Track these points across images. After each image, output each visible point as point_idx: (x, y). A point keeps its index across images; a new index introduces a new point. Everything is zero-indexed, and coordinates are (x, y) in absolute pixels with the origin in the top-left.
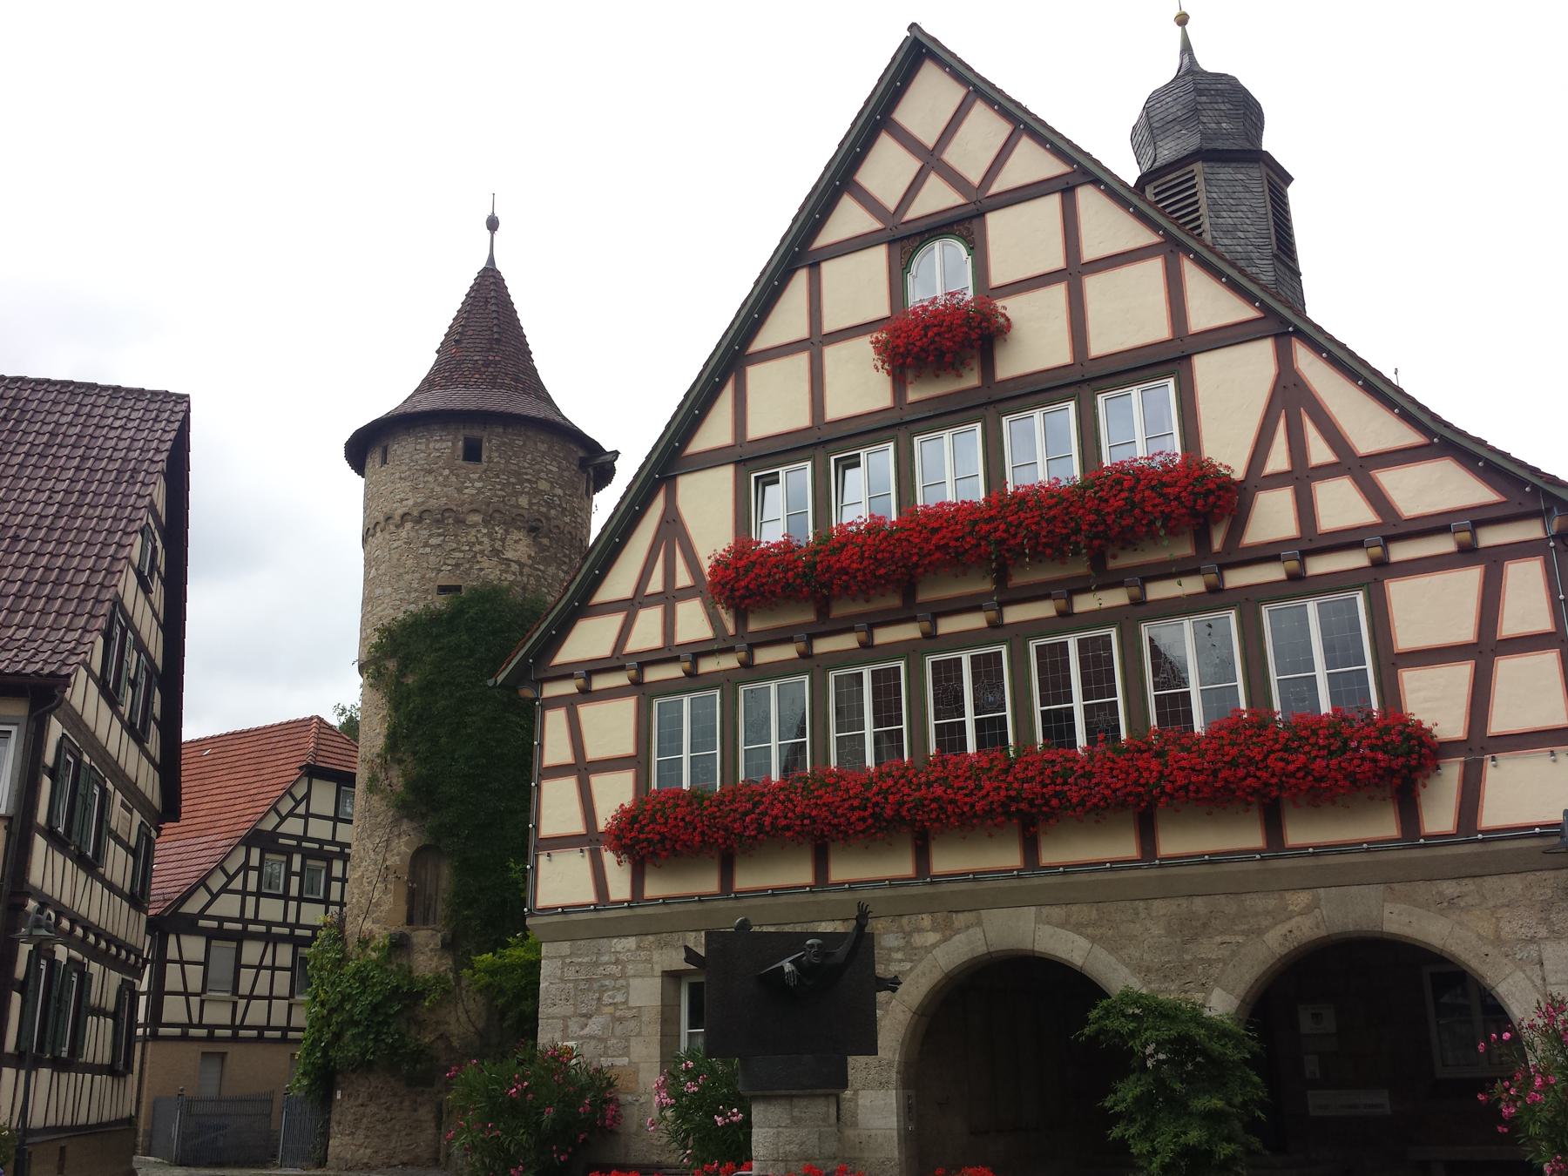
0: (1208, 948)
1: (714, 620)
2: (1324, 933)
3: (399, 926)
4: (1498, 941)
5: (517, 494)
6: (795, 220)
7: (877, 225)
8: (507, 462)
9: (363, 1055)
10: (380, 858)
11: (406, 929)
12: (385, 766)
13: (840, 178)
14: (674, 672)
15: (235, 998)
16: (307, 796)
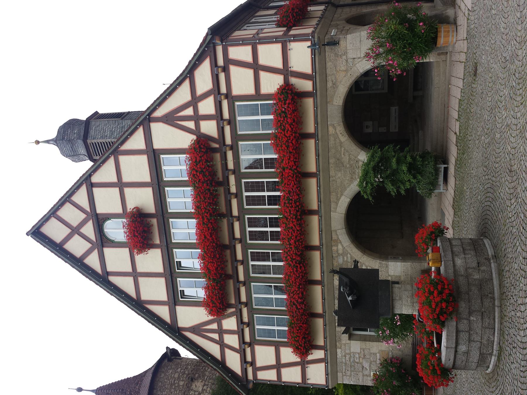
0: (345, 159)
2: (342, 123)
4: (346, 71)
5: (179, 386)
6: (91, 280)
7: (96, 251)
8: (167, 389)
13: (78, 263)
14: (247, 331)
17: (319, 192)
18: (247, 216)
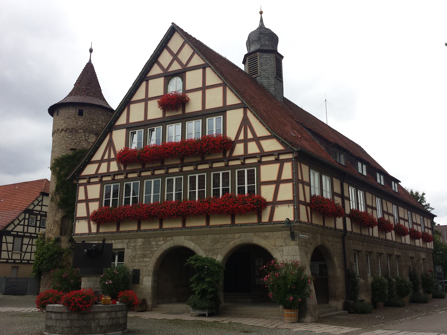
0: (218, 246)
1: (119, 168)
3: (58, 235)
4: (275, 246)
5: (92, 125)
6: (143, 69)
7: (162, 72)
9: (48, 267)
10: (53, 218)
11: (60, 236)
12: (55, 195)
14: (109, 178)
16: (42, 200)
17: (197, 227)
18: (205, 174)
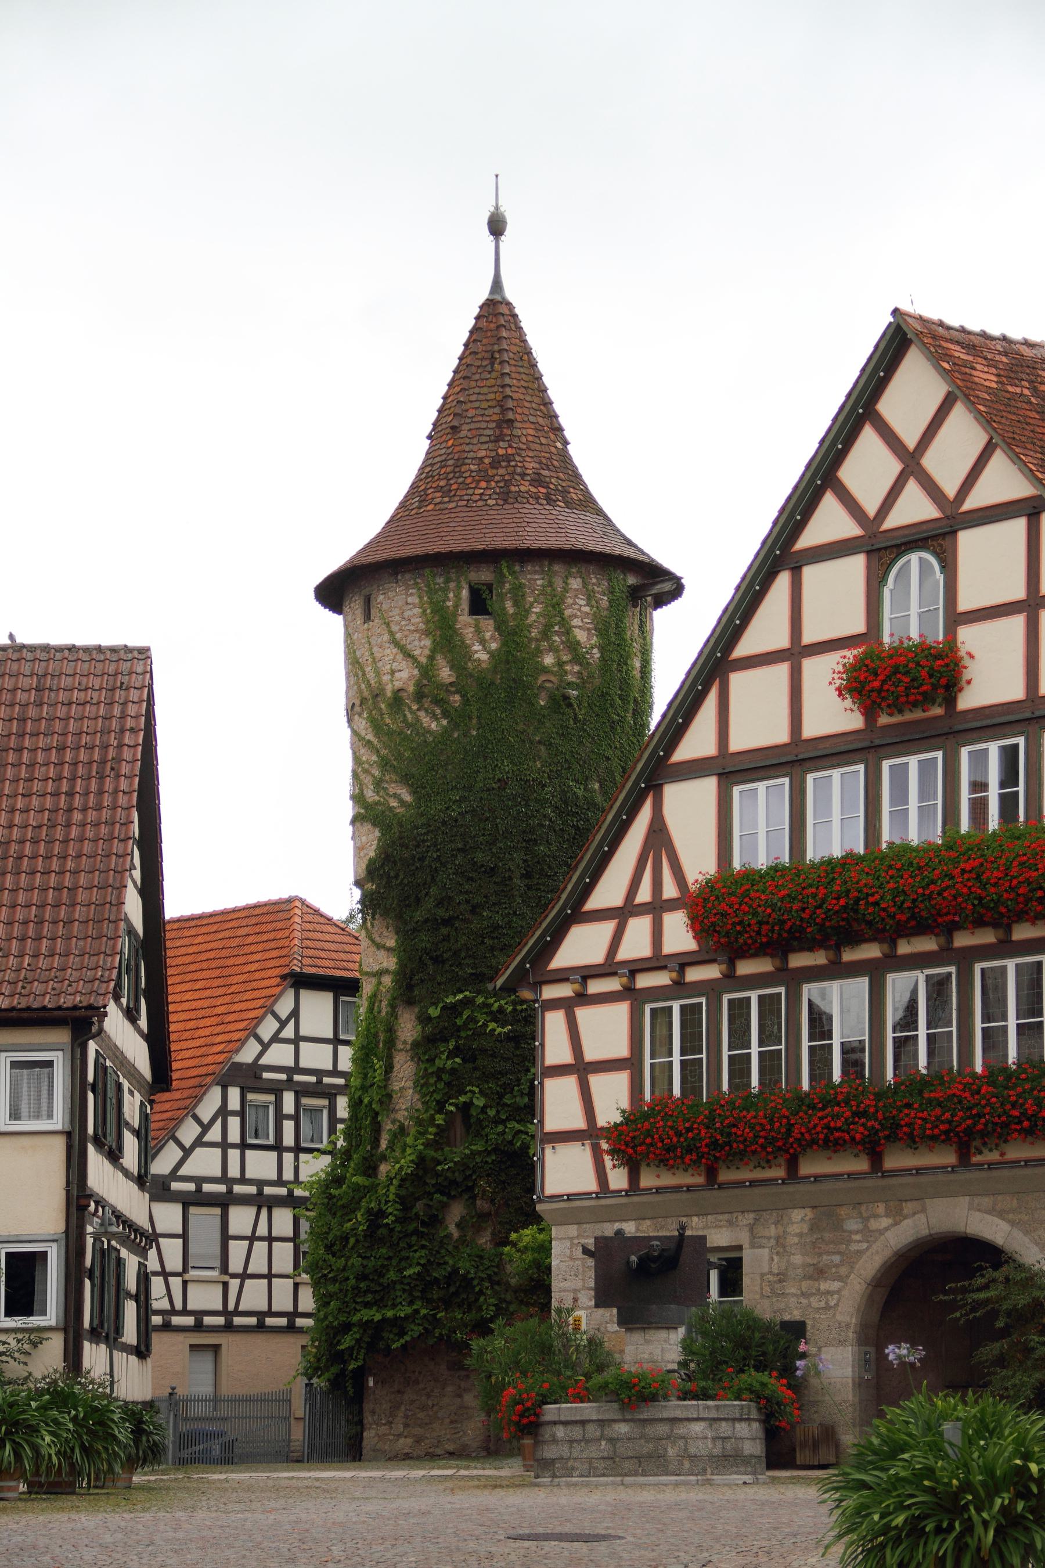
14: (662, 979)
15: (226, 1278)
